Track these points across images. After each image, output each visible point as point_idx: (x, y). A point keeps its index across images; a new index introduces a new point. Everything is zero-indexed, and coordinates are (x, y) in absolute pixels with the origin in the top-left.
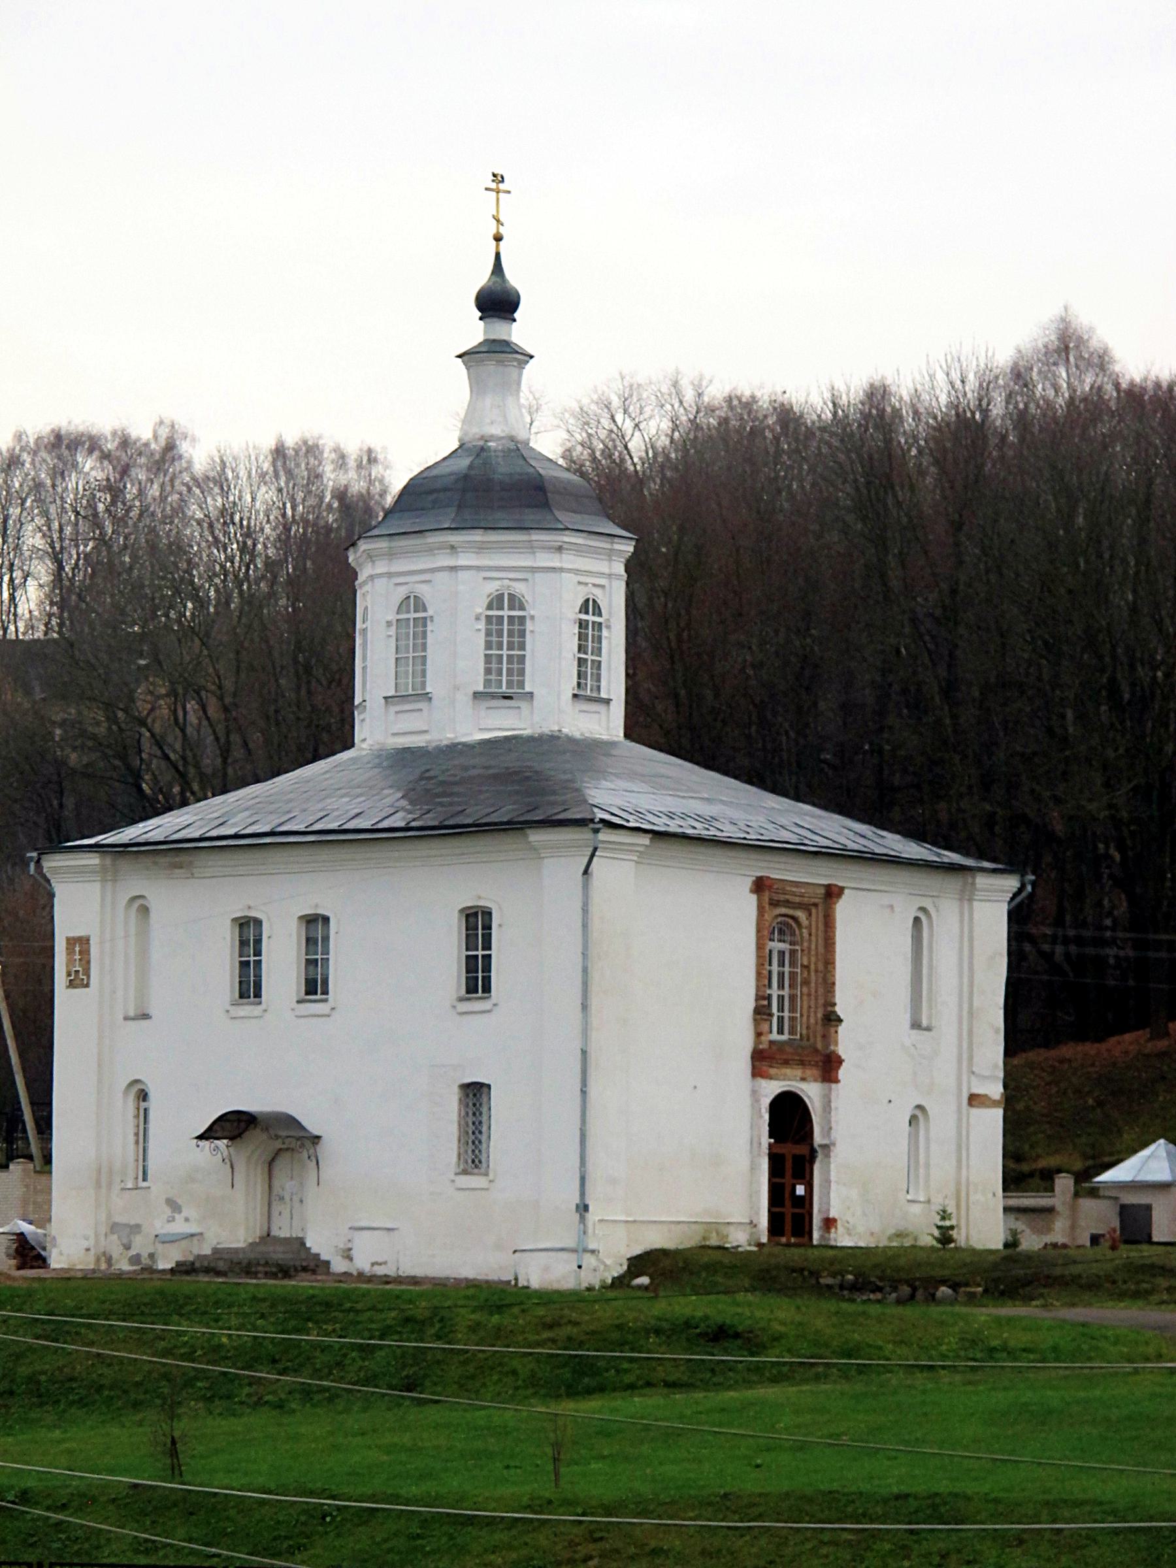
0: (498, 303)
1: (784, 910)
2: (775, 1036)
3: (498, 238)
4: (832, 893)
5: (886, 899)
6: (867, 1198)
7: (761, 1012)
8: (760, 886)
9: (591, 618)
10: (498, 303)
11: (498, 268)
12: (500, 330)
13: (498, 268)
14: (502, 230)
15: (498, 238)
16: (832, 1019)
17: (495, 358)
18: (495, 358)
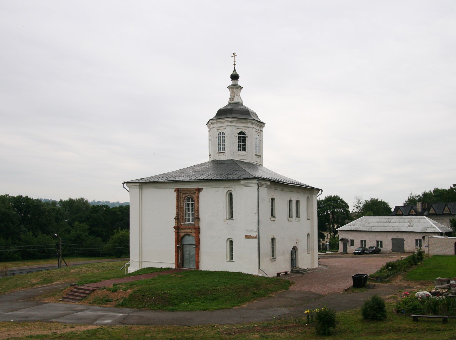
0: (235, 77)
1: (188, 195)
2: (191, 222)
3: (235, 65)
4: (199, 190)
5: (217, 189)
6: (212, 259)
7: (177, 218)
8: (177, 190)
9: (221, 136)
10: (235, 77)
11: (235, 70)
12: (235, 82)
13: (235, 70)
14: (235, 63)
15: (235, 65)
16: (198, 219)
17: (235, 88)
18: (235, 88)
